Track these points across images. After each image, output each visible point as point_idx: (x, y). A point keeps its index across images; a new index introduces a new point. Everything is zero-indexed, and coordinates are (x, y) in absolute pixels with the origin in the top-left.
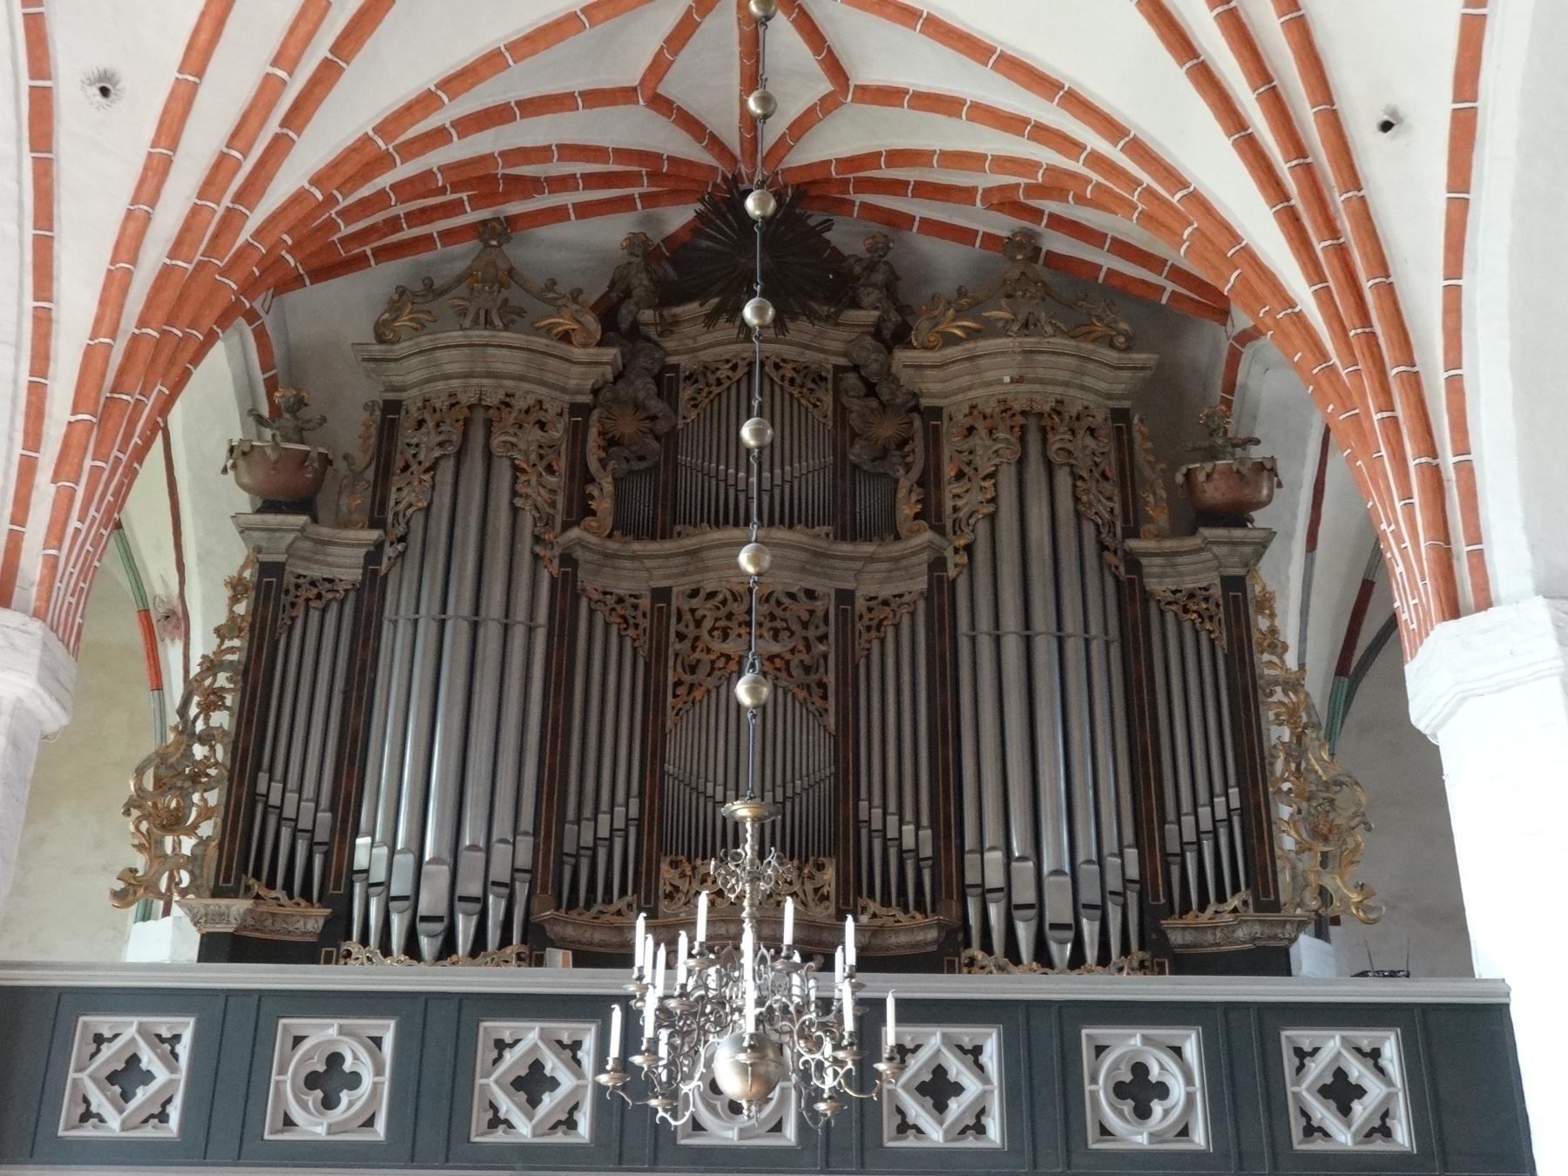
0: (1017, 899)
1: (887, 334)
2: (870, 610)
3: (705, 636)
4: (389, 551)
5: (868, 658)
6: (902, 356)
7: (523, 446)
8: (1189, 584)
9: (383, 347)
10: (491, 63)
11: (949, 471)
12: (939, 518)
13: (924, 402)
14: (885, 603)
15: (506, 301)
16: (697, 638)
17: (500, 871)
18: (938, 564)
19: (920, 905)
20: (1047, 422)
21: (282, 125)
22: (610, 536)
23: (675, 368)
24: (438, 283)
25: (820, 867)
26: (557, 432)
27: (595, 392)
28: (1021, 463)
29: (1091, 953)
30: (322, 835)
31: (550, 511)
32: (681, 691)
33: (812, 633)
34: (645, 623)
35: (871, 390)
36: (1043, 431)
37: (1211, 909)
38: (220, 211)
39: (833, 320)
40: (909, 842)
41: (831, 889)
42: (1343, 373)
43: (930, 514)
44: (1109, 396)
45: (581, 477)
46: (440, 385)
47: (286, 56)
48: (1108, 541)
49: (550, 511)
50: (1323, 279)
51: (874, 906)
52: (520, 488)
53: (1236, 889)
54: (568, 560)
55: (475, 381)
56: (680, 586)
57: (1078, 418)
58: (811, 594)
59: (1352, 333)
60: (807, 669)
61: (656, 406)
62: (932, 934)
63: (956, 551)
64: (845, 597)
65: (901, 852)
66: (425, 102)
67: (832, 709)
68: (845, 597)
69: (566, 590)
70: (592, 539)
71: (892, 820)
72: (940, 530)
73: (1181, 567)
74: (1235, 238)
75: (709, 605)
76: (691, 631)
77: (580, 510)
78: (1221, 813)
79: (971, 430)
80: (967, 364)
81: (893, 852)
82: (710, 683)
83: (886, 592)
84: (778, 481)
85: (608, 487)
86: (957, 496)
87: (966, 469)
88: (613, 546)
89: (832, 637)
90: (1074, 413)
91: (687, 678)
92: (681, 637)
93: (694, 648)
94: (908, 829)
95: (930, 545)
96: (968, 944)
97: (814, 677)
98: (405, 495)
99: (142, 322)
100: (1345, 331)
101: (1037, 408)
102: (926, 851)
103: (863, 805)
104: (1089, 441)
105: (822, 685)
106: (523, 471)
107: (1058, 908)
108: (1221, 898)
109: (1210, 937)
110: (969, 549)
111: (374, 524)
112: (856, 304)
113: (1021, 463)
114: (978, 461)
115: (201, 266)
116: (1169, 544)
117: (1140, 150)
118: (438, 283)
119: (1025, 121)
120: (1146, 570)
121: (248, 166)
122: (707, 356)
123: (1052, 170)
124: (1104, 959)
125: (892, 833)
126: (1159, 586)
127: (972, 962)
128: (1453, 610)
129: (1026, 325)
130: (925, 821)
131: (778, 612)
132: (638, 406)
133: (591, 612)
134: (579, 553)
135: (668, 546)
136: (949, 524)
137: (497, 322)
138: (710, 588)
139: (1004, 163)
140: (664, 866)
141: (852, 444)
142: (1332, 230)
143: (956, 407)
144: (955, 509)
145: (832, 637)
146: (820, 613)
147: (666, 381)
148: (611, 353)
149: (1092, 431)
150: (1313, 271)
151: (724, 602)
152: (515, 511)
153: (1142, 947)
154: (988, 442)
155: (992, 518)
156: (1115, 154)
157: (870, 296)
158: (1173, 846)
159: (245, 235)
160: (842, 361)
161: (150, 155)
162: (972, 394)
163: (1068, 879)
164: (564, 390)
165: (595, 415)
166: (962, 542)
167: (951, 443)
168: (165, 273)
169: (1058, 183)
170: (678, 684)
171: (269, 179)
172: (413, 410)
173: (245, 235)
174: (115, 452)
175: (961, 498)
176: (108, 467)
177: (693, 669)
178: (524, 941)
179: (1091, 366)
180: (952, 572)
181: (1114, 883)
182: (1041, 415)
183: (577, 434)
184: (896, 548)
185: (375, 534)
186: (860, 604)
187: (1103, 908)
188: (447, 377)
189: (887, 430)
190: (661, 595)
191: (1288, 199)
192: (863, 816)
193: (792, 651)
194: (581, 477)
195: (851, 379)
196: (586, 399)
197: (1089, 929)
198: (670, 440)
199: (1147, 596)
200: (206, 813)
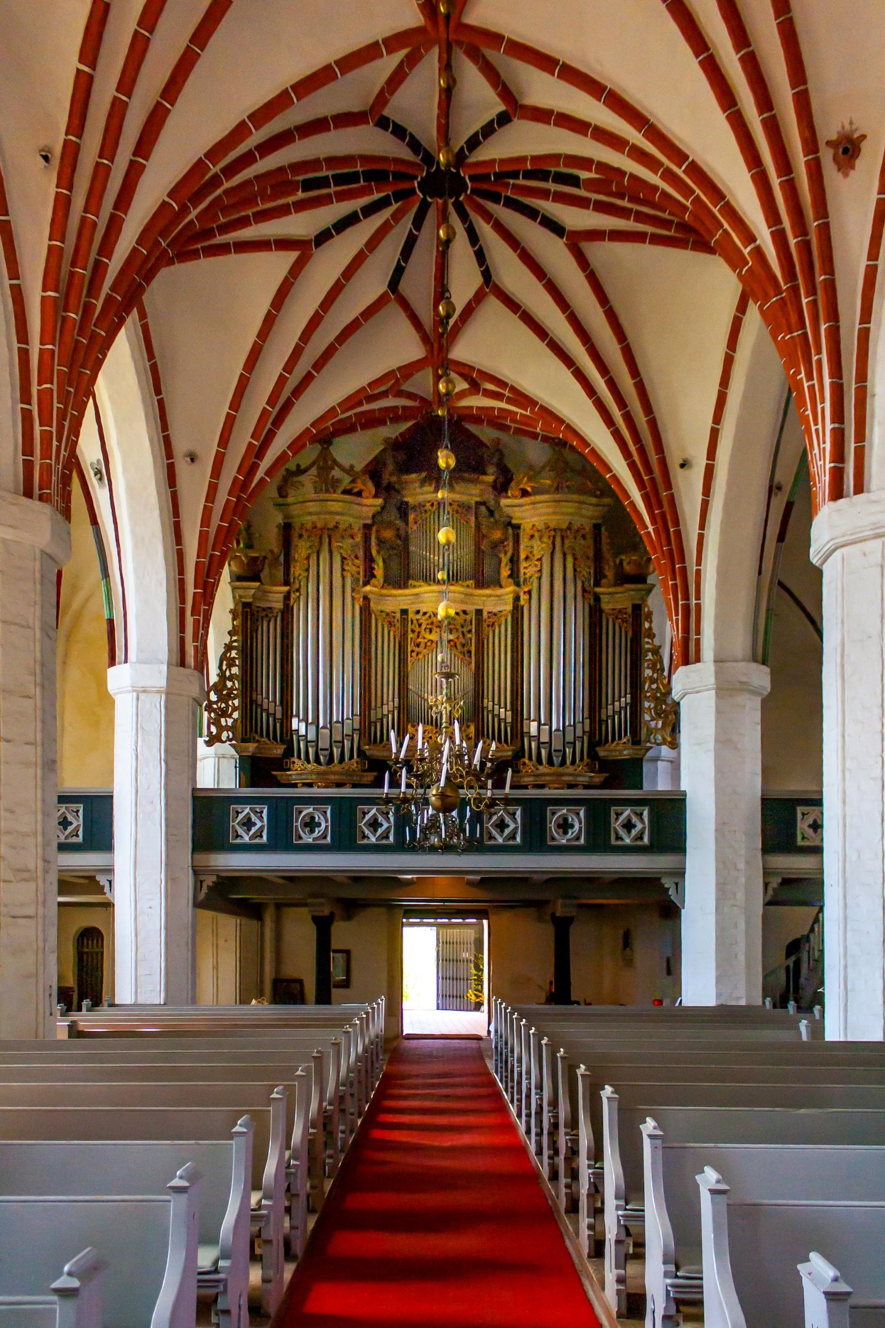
0: (542, 740)
1: (498, 485)
2: (489, 617)
3: (423, 632)
4: (293, 596)
5: (488, 638)
6: (504, 502)
7: (345, 547)
8: (619, 607)
9: (282, 499)
11: (522, 556)
12: (518, 576)
13: (514, 522)
14: (495, 615)
15: (333, 477)
16: (419, 632)
18: (517, 599)
19: (506, 741)
20: (564, 534)
22: (383, 587)
23: (407, 503)
24: (303, 467)
25: (468, 727)
26: (359, 538)
27: (374, 517)
28: (552, 554)
30: (279, 715)
31: (357, 576)
32: (414, 654)
33: (465, 630)
34: (398, 625)
35: (491, 513)
36: (563, 538)
37: (615, 743)
40: (502, 716)
41: (472, 735)
43: (514, 575)
44: (592, 518)
45: (369, 560)
46: (309, 518)
48: (587, 588)
49: (357, 576)
52: (346, 568)
53: (626, 734)
54: (366, 598)
55: (322, 516)
56: (412, 609)
57: (578, 531)
58: (465, 612)
60: (463, 646)
62: (510, 753)
63: (525, 593)
64: (479, 612)
65: (499, 720)
67: (473, 661)
68: (479, 612)
69: (366, 611)
70: (375, 589)
71: (496, 707)
72: (517, 584)
75: (424, 618)
76: (417, 629)
78: (623, 705)
79: (532, 536)
80: (531, 506)
81: (496, 720)
82: (425, 651)
83: (495, 610)
84: (451, 561)
85: (381, 564)
86: (525, 568)
87: (530, 555)
88: (384, 592)
89: (473, 630)
90: (576, 528)
91: (417, 649)
92: (413, 631)
93: (418, 636)
94: (502, 710)
96: (524, 757)
97: (466, 649)
98: (297, 570)
101: (561, 527)
102: (509, 720)
103: (485, 701)
104: (582, 542)
105: (470, 652)
106: (346, 559)
108: (620, 738)
109: (614, 754)
110: (529, 592)
111: (286, 583)
112: (485, 473)
113: (552, 554)
114: (535, 552)
116: (611, 590)
118: (303, 467)
120: (602, 600)
122: (421, 498)
125: (496, 712)
127: (524, 764)
129: (557, 489)
130: (508, 708)
131: (452, 622)
132: (390, 525)
133: (376, 620)
134: (370, 596)
135: (406, 591)
136: (522, 580)
137: (331, 490)
138: (425, 611)
140: (409, 727)
141: (483, 539)
144: (525, 574)
145: (473, 630)
146: (469, 620)
147: (403, 510)
148: (379, 501)
149: (584, 537)
151: (430, 617)
152: (343, 578)
153: (588, 757)
154: (539, 543)
155: (540, 578)
157: (491, 469)
158: (604, 717)
160: (478, 499)
162: (533, 520)
163: (561, 733)
164: (360, 517)
165: (374, 529)
166: (526, 589)
167: (524, 543)
170: (412, 651)
172: (297, 528)
175: (527, 569)
177: (418, 645)
178: (358, 756)
179: (584, 506)
180: (522, 602)
181: (579, 733)
182: (561, 530)
183: (367, 539)
184: (499, 591)
185: (286, 588)
186: (485, 614)
187: (574, 743)
188: (310, 514)
189: (497, 535)
190: (404, 612)
192: (485, 705)
193: (458, 638)
195: (483, 508)
196: (369, 522)
198: (405, 540)
199: (601, 611)
200: (235, 709)
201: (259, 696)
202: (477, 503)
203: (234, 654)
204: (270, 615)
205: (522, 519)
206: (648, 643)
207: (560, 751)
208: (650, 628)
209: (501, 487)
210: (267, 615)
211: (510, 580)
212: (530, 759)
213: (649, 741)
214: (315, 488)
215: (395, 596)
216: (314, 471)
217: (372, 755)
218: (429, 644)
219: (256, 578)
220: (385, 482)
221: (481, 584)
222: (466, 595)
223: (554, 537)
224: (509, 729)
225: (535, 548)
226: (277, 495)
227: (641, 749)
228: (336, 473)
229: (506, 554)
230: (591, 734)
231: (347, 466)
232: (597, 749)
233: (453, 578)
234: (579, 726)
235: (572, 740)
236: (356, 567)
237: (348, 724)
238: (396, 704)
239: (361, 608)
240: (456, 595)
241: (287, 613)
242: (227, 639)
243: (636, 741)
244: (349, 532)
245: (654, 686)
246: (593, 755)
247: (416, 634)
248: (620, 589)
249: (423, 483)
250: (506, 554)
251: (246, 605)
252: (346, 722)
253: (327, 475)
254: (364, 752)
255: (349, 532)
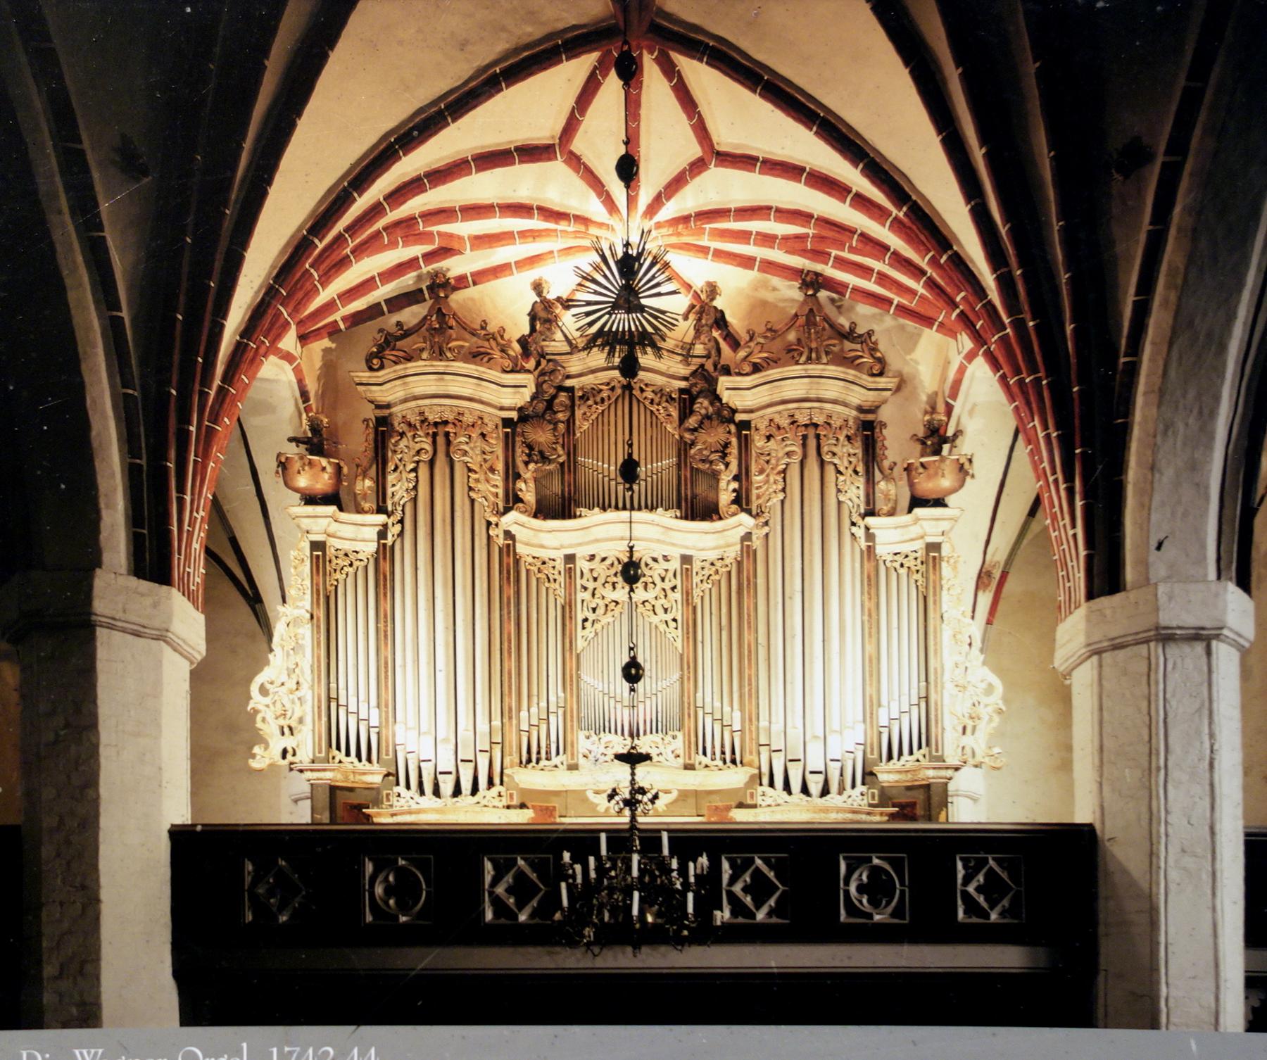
34: (561, 579)
44: (860, 409)
56: (581, 552)
58: (666, 558)
60: (666, 611)
64: (686, 559)
76: (591, 585)
77: (512, 500)
89: (679, 587)
111: (381, 510)
145: (679, 587)
185: (382, 518)
190: (570, 558)
194: (512, 475)
236: (492, 487)
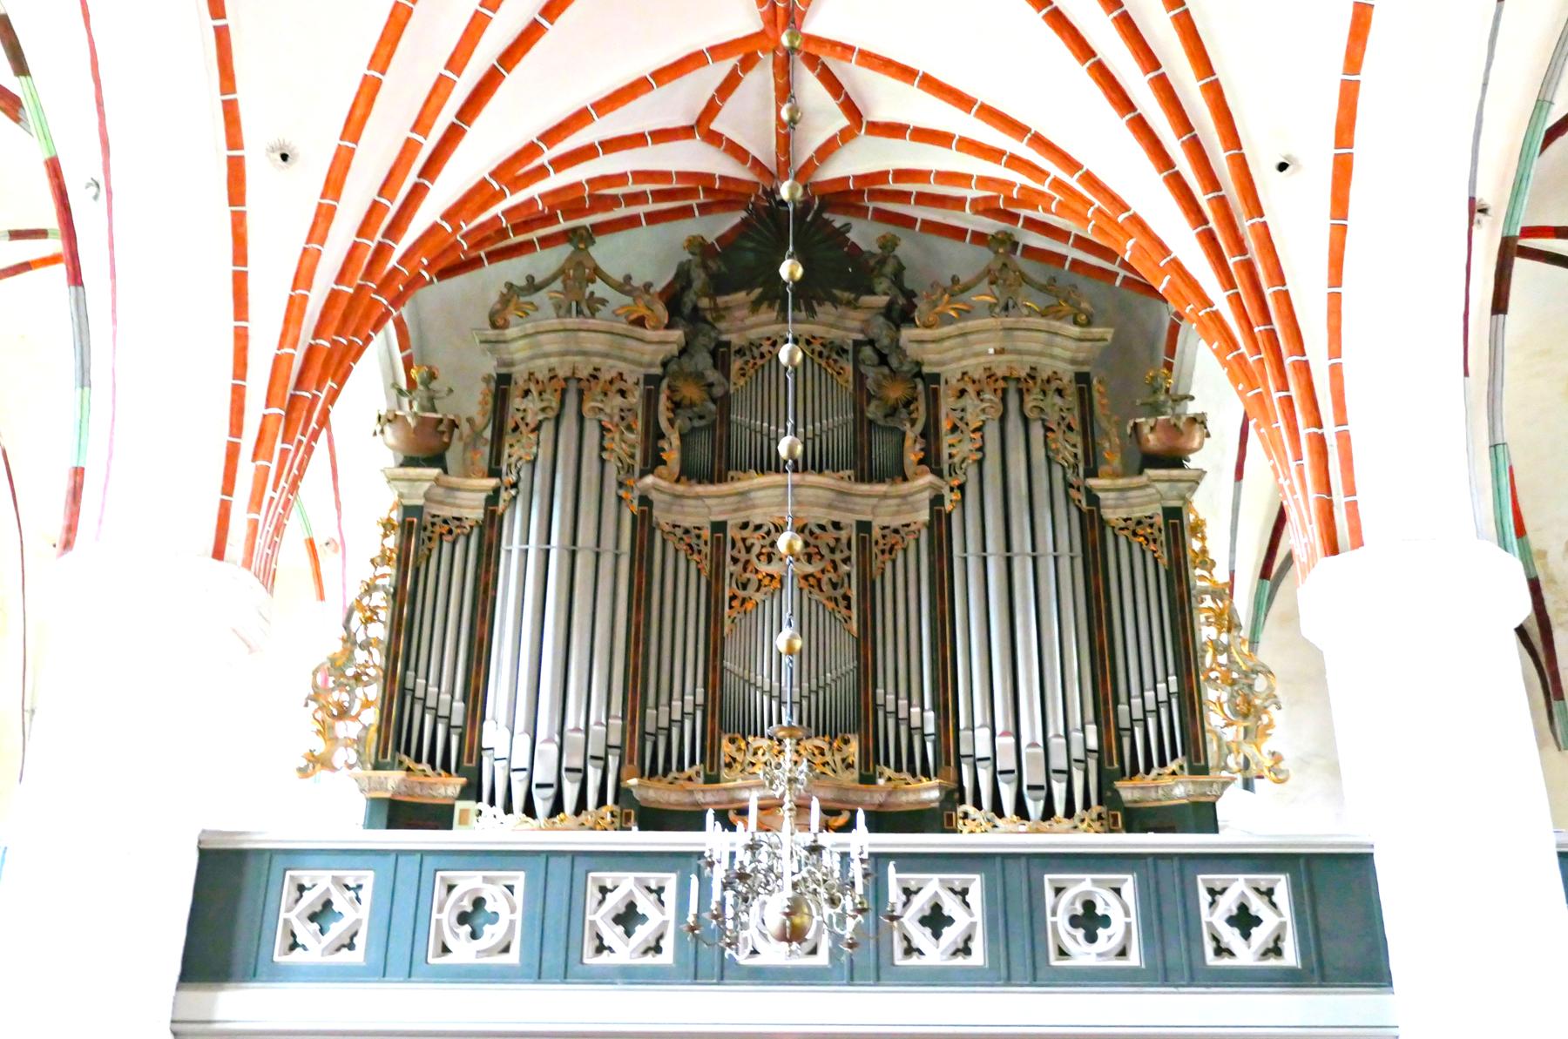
1: (895, 314)
2: (884, 537)
3: (754, 560)
4: (504, 495)
6: (907, 334)
7: (608, 410)
8: (1137, 514)
10: (580, 119)
11: (945, 425)
13: (926, 370)
14: (896, 531)
15: (592, 293)
16: (747, 562)
17: (596, 749)
18: (937, 500)
20: (1023, 386)
21: (421, 175)
22: (678, 481)
23: (728, 344)
24: (538, 280)
25: (846, 742)
26: (636, 398)
27: (664, 365)
28: (1003, 420)
29: (1060, 807)
30: (457, 720)
32: (736, 603)
33: (838, 557)
34: (706, 550)
35: (883, 360)
36: (1020, 392)
37: (1154, 772)
38: (373, 245)
39: (852, 305)
40: (916, 722)
42: (1251, 360)
43: (931, 460)
44: (1073, 362)
45: (654, 435)
46: (541, 362)
47: (422, 124)
50: (1233, 286)
51: (889, 772)
52: (606, 444)
53: (1174, 756)
54: (645, 501)
55: (569, 358)
56: (733, 520)
57: (1048, 381)
58: (836, 525)
59: (1256, 330)
60: (835, 586)
61: (713, 375)
62: (935, 794)
63: (952, 490)
64: (864, 527)
65: (910, 729)
66: (530, 150)
68: (864, 527)
69: (644, 523)
70: (663, 484)
71: (903, 703)
72: (938, 473)
73: (1128, 499)
74: (1166, 251)
76: (743, 556)
77: (654, 461)
78: (1163, 697)
79: (962, 392)
80: (959, 340)
81: (903, 729)
82: (758, 597)
83: (896, 522)
84: (810, 435)
85: (676, 441)
86: (951, 446)
87: (959, 424)
88: (680, 488)
90: (1045, 377)
91: (741, 593)
92: (735, 560)
93: (745, 570)
95: (931, 486)
97: (840, 592)
98: (516, 451)
99: (317, 334)
100: (1251, 328)
101: (1016, 374)
102: (930, 728)
103: (880, 691)
104: (1057, 400)
105: (847, 598)
106: (609, 430)
107: (1033, 774)
108: (1163, 763)
109: (1153, 795)
110: (962, 488)
111: (494, 472)
112: (871, 292)
113: (1003, 420)
114: (968, 417)
115: (360, 288)
116: (1121, 482)
117: (1090, 180)
118: (538, 280)
119: (1002, 153)
120: (1102, 503)
121: (394, 208)
122: (753, 334)
123: (1023, 188)
124: (1070, 812)
125: (903, 714)
126: (1112, 514)
127: (966, 815)
128: (1333, 549)
129: (1006, 308)
130: (927, 704)
131: (811, 540)
132: (699, 376)
133: (664, 541)
134: (654, 496)
137: (586, 311)
138: (758, 522)
139: (984, 182)
140: (725, 741)
142: (1239, 246)
143: (951, 373)
144: (951, 456)
146: (844, 541)
147: (721, 355)
148: (677, 335)
149: (1060, 392)
150: (1228, 281)
151: (768, 533)
152: (603, 461)
153: (1100, 803)
154: (977, 402)
155: (980, 463)
156: (1073, 181)
157: (883, 284)
158: (1124, 722)
159: (393, 262)
160: (860, 337)
161: (320, 205)
162: (964, 363)
163: (1041, 751)
164: (640, 364)
165: (664, 384)
166: (955, 483)
167: (947, 403)
168: (334, 296)
169: (1030, 198)
170: (733, 597)
171: (410, 218)
173: (393, 262)
174: (298, 436)
176: (292, 448)
177: (744, 587)
178: (616, 802)
180: (948, 506)
181: (1077, 753)
182: (1018, 380)
183: (650, 400)
184: (904, 488)
185: (492, 482)
186: (876, 533)
187: (1069, 773)
188: (546, 355)
189: (896, 393)
190: (719, 527)
191: (1206, 222)
192: (880, 701)
193: (823, 571)
194: (654, 435)
195: (867, 351)
196: (658, 371)
197: (1059, 790)
198: (724, 403)
199: (1103, 523)
200: (367, 704)
201: (421, 681)
202: (857, 344)
203: (379, 599)
204: (456, 531)
205: (943, 364)
206: (1202, 578)
207: (1040, 788)
208: (1204, 551)
209: (900, 314)
210: (450, 532)
211: (925, 468)
212: (978, 804)
213: (1226, 767)
214: (558, 307)
215: (698, 497)
216: (558, 285)
217: (646, 800)
218: (766, 581)
219: (436, 459)
220: (687, 310)
221: (867, 474)
222: (840, 493)
223: (1005, 391)
224: (929, 747)
225: (969, 410)
226: (487, 324)
227: (1211, 784)
228: (599, 289)
229: (913, 425)
230: (1101, 753)
231: (617, 275)
232: (1118, 784)
233: (810, 463)
234: (1076, 736)
235: (1064, 767)
237: (596, 732)
238: (700, 700)
239: (634, 517)
240: (820, 492)
241: (492, 524)
242: (368, 572)
243: (1198, 767)
244: (618, 385)
245: (1223, 659)
246: (1107, 796)
247: (740, 565)
248: (1137, 481)
249: (755, 306)
250: (913, 425)
251: (408, 511)
252: (593, 727)
253: (582, 289)
254: (629, 791)
255: (618, 385)
